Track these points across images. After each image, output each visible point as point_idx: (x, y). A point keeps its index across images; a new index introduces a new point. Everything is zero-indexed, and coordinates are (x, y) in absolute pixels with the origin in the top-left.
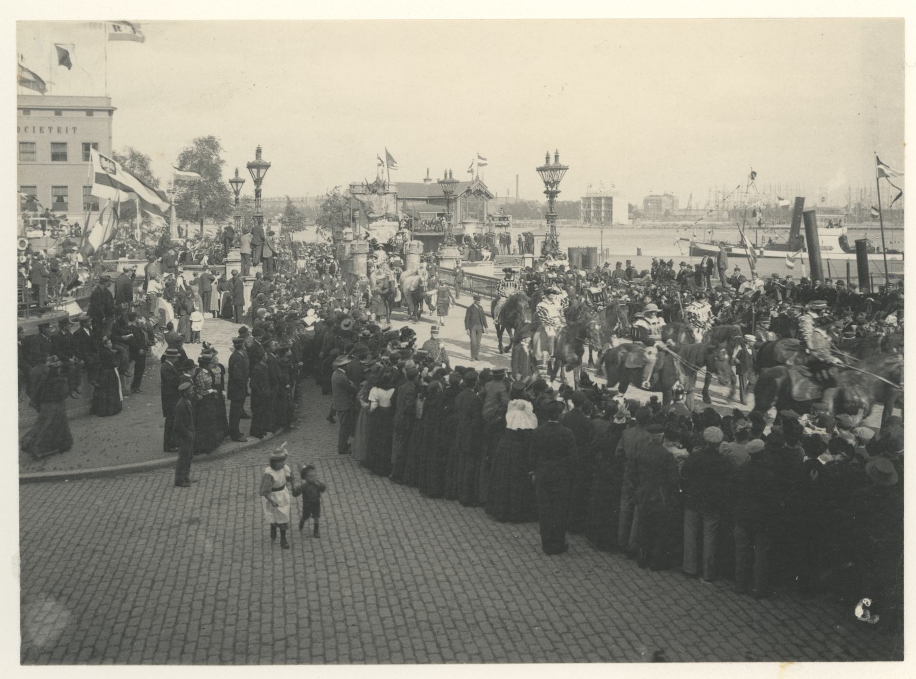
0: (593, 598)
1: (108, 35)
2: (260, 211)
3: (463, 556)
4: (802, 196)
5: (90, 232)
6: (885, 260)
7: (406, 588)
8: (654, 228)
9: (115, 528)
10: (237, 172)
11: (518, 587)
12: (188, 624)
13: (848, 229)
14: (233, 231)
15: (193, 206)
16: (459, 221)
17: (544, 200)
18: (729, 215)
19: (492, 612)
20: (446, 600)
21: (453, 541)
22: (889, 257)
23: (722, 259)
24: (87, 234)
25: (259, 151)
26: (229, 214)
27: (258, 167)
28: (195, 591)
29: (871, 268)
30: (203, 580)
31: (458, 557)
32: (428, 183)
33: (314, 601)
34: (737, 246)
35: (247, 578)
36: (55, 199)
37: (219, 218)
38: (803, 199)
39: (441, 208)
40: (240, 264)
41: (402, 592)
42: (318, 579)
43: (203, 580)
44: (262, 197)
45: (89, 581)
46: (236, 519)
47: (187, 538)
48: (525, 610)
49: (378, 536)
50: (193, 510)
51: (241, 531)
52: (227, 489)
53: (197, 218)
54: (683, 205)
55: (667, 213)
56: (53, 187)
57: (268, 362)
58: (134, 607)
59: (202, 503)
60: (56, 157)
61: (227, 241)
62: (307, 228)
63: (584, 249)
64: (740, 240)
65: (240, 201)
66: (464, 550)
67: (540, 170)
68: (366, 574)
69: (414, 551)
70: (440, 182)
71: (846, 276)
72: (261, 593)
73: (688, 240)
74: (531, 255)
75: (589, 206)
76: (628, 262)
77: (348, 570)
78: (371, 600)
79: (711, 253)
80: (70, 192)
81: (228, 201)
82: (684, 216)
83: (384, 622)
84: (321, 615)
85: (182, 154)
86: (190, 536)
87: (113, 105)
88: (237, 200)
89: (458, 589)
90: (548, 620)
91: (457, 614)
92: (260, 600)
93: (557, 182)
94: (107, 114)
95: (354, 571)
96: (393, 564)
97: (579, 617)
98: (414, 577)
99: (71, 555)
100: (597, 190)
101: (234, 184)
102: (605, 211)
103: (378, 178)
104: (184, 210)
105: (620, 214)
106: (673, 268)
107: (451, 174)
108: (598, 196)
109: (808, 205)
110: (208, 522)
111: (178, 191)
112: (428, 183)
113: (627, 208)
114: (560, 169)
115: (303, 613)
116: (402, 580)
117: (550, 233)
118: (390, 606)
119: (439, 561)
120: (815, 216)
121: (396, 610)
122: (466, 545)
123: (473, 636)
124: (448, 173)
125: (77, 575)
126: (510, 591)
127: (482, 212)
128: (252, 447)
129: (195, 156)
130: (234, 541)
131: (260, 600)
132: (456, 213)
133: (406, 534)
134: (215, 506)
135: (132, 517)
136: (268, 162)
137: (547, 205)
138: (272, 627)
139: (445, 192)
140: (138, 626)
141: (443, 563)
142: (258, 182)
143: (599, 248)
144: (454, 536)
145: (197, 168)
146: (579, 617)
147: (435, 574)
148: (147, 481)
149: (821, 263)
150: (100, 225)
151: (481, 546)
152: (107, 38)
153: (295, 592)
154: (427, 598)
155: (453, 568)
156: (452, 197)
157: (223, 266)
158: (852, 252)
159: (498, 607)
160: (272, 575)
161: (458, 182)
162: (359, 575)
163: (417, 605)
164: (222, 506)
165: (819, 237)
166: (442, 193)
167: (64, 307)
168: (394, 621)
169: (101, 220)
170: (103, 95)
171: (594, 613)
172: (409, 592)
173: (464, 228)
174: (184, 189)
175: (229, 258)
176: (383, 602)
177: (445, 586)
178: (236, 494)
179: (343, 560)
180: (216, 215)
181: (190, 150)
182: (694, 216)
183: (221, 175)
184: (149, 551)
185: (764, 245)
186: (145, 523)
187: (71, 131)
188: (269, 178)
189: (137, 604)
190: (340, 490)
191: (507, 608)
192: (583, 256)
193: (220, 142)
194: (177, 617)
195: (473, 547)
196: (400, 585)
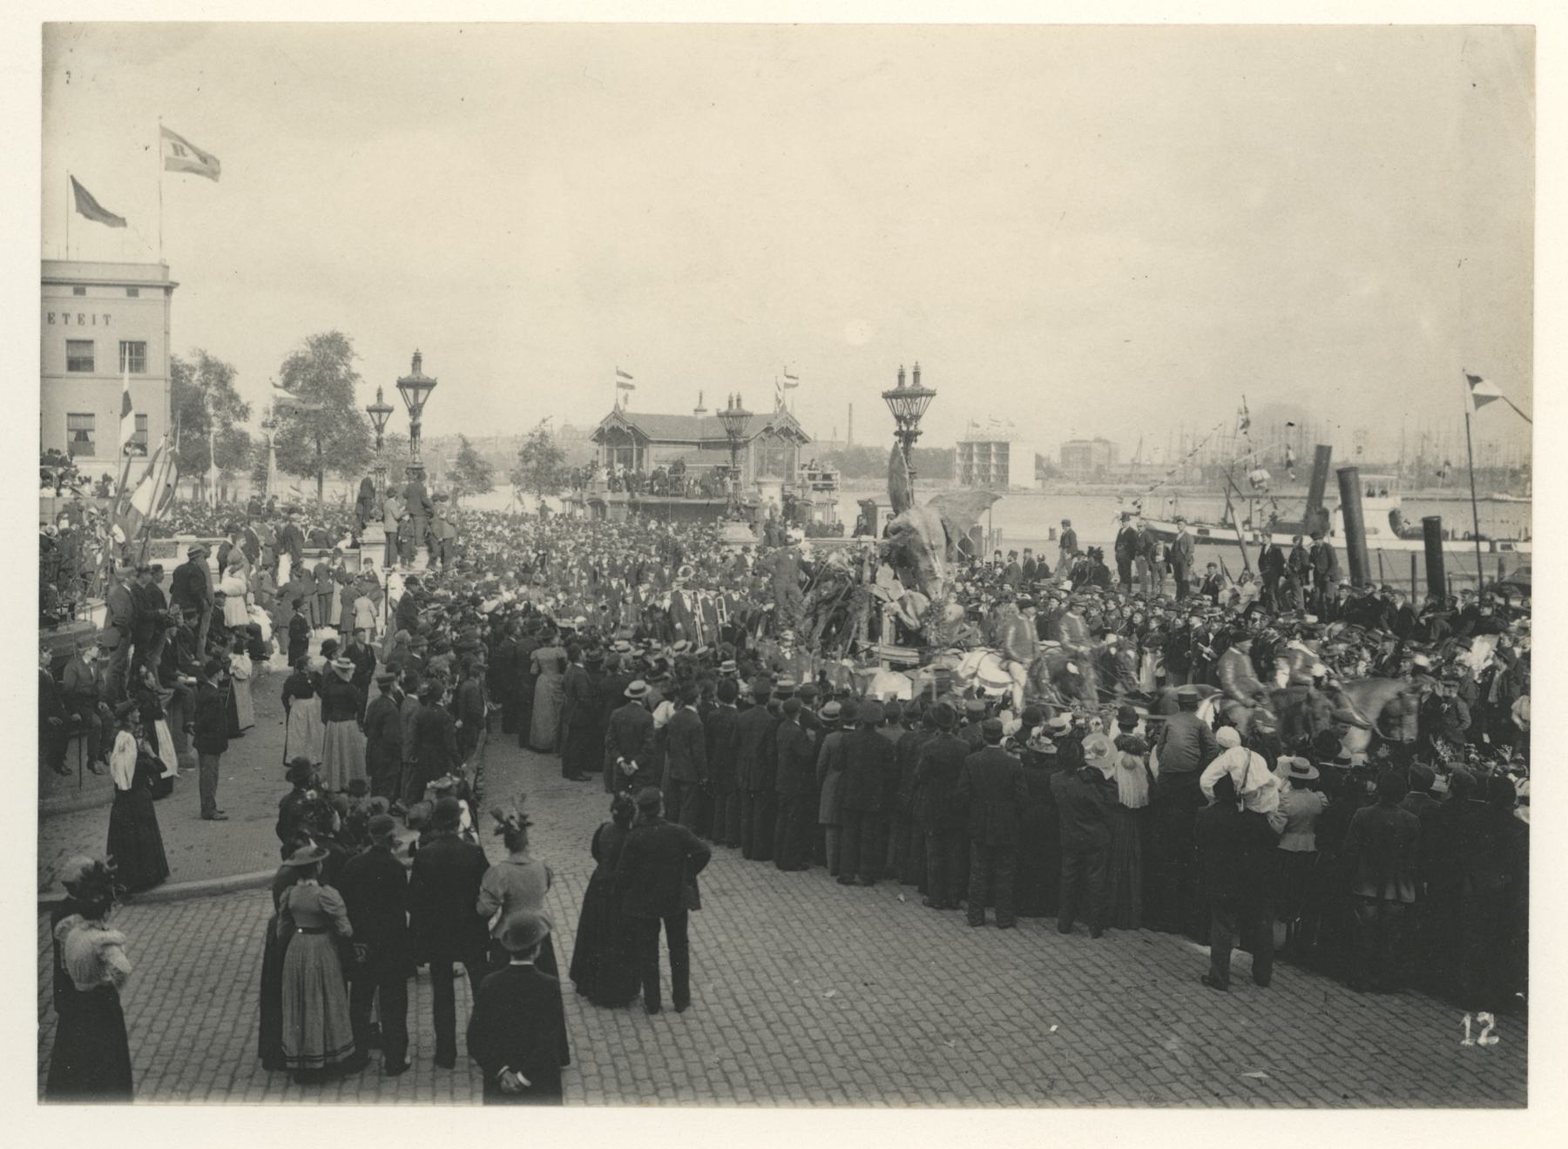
9: (170, 988)
10: (380, 394)
13: (1403, 500)
15: (305, 450)
16: (751, 479)
18: (1203, 476)
21: (735, 1013)
24: (123, 491)
25: (417, 359)
26: (366, 463)
27: (416, 385)
31: (744, 1042)
32: (701, 416)
36: (73, 435)
37: (348, 471)
38: (1330, 448)
39: (722, 457)
44: (422, 436)
53: (311, 470)
54: (1125, 458)
60: (74, 365)
64: (1222, 516)
65: (385, 443)
66: (754, 1031)
67: (887, 396)
69: (670, 1030)
70: (720, 416)
71: (1409, 576)
74: (871, 538)
75: (970, 457)
79: (1169, 537)
80: (98, 422)
81: (365, 441)
82: (1129, 476)
85: (289, 362)
87: (172, 277)
88: (379, 442)
93: (917, 417)
94: (162, 291)
101: (375, 415)
102: (997, 466)
103: (617, 406)
104: (293, 462)
105: (1021, 472)
108: (985, 440)
109: (1337, 459)
111: (281, 424)
113: (1033, 460)
114: (922, 395)
120: (1357, 478)
124: (735, 399)
127: (790, 467)
129: (310, 366)
132: (747, 467)
135: (197, 971)
139: (729, 432)
142: (415, 411)
144: (739, 1006)
148: (223, 909)
152: (163, 165)
156: (741, 440)
161: (751, 415)
166: (725, 434)
167: (88, 616)
170: (156, 261)
173: (760, 491)
181: (300, 355)
182: (1144, 476)
183: (352, 398)
184: (226, 1027)
186: (220, 980)
187: (100, 320)
188: (433, 404)
195: (769, 1025)
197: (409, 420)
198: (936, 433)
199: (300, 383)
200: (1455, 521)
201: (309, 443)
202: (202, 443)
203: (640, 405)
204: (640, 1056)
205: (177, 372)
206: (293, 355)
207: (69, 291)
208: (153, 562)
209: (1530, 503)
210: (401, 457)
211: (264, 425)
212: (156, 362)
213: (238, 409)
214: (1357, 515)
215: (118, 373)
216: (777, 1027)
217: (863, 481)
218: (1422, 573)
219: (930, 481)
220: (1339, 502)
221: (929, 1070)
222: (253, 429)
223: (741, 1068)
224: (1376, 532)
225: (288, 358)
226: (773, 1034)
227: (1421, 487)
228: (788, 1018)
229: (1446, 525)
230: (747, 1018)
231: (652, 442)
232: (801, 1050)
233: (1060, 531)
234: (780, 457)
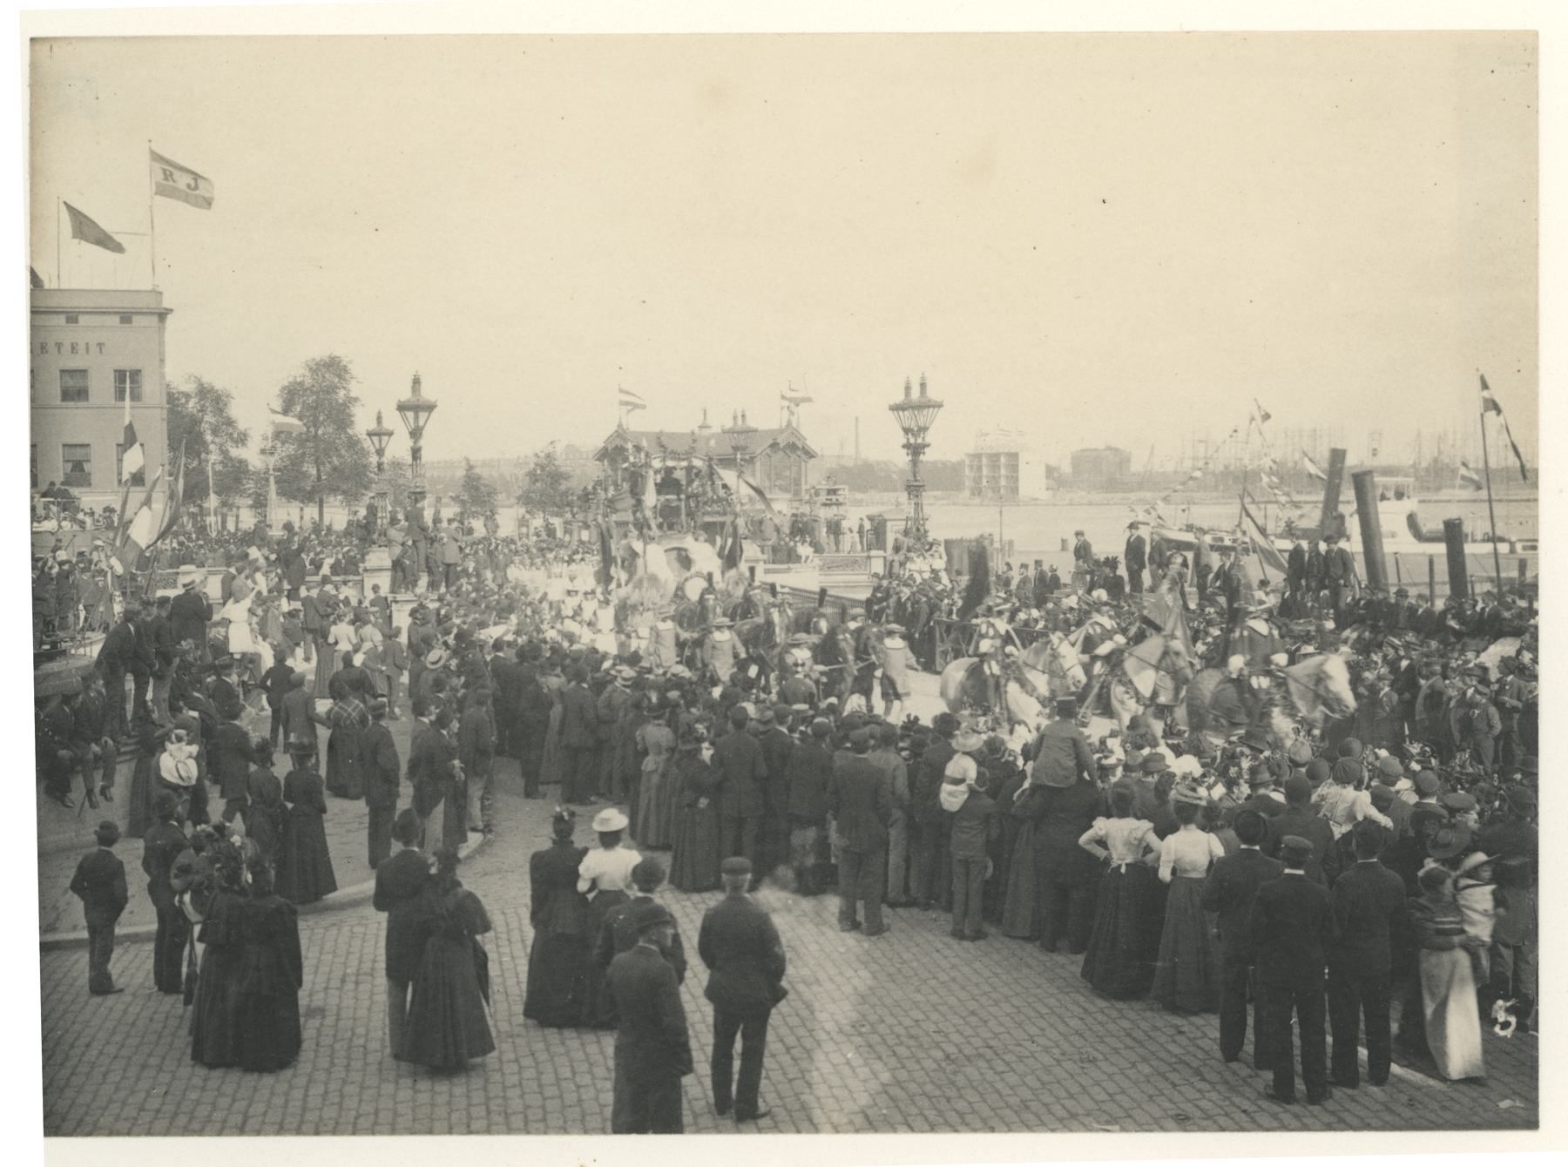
1: (154, 188)
4: (1339, 446)
5: (131, 522)
8: (1090, 504)
10: (379, 419)
15: (305, 475)
17: (902, 459)
25: (416, 382)
26: (366, 488)
27: (416, 408)
29: (1471, 568)
32: (706, 432)
36: (70, 465)
37: (351, 497)
38: (1344, 452)
40: (389, 574)
42: (527, 1107)
44: (423, 460)
45: (136, 1119)
52: (372, 957)
54: (1136, 466)
56: (64, 446)
59: (329, 980)
60: (67, 395)
63: (970, 541)
67: (896, 408)
71: (1427, 580)
73: (1147, 524)
74: (881, 553)
75: (980, 468)
76: (1038, 563)
79: (1188, 546)
80: (95, 452)
85: (284, 388)
87: (166, 304)
88: (380, 465)
93: (924, 429)
94: (155, 319)
99: (105, 1075)
101: (375, 439)
102: (1007, 477)
103: (620, 425)
104: (292, 485)
105: (1032, 482)
109: (1352, 461)
110: (338, 1014)
111: (279, 450)
117: (912, 515)
125: (115, 1108)
127: (797, 482)
134: (350, 986)
136: (433, 400)
137: (908, 468)
142: (416, 434)
143: (996, 538)
149: (1383, 563)
161: (756, 431)
162: (597, 1099)
164: (361, 987)
167: (88, 649)
169: (147, 502)
174: (291, 449)
175: (368, 565)
181: (299, 380)
185: (1279, 531)
187: (94, 349)
193: (350, 366)
195: (788, 1050)
197: (410, 443)
198: (944, 445)
199: (299, 408)
202: (201, 471)
203: (638, 423)
205: (172, 398)
206: (291, 379)
207: (62, 319)
210: (401, 481)
211: (263, 452)
213: (235, 436)
214: (1373, 516)
217: (875, 495)
219: (938, 493)
220: (1355, 506)
221: (952, 1093)
222: (251, 455)
224: (1393, 535)
225: (286, 384)
229: (1467, 528)
233: (1073, 543)
234: (787, 473)
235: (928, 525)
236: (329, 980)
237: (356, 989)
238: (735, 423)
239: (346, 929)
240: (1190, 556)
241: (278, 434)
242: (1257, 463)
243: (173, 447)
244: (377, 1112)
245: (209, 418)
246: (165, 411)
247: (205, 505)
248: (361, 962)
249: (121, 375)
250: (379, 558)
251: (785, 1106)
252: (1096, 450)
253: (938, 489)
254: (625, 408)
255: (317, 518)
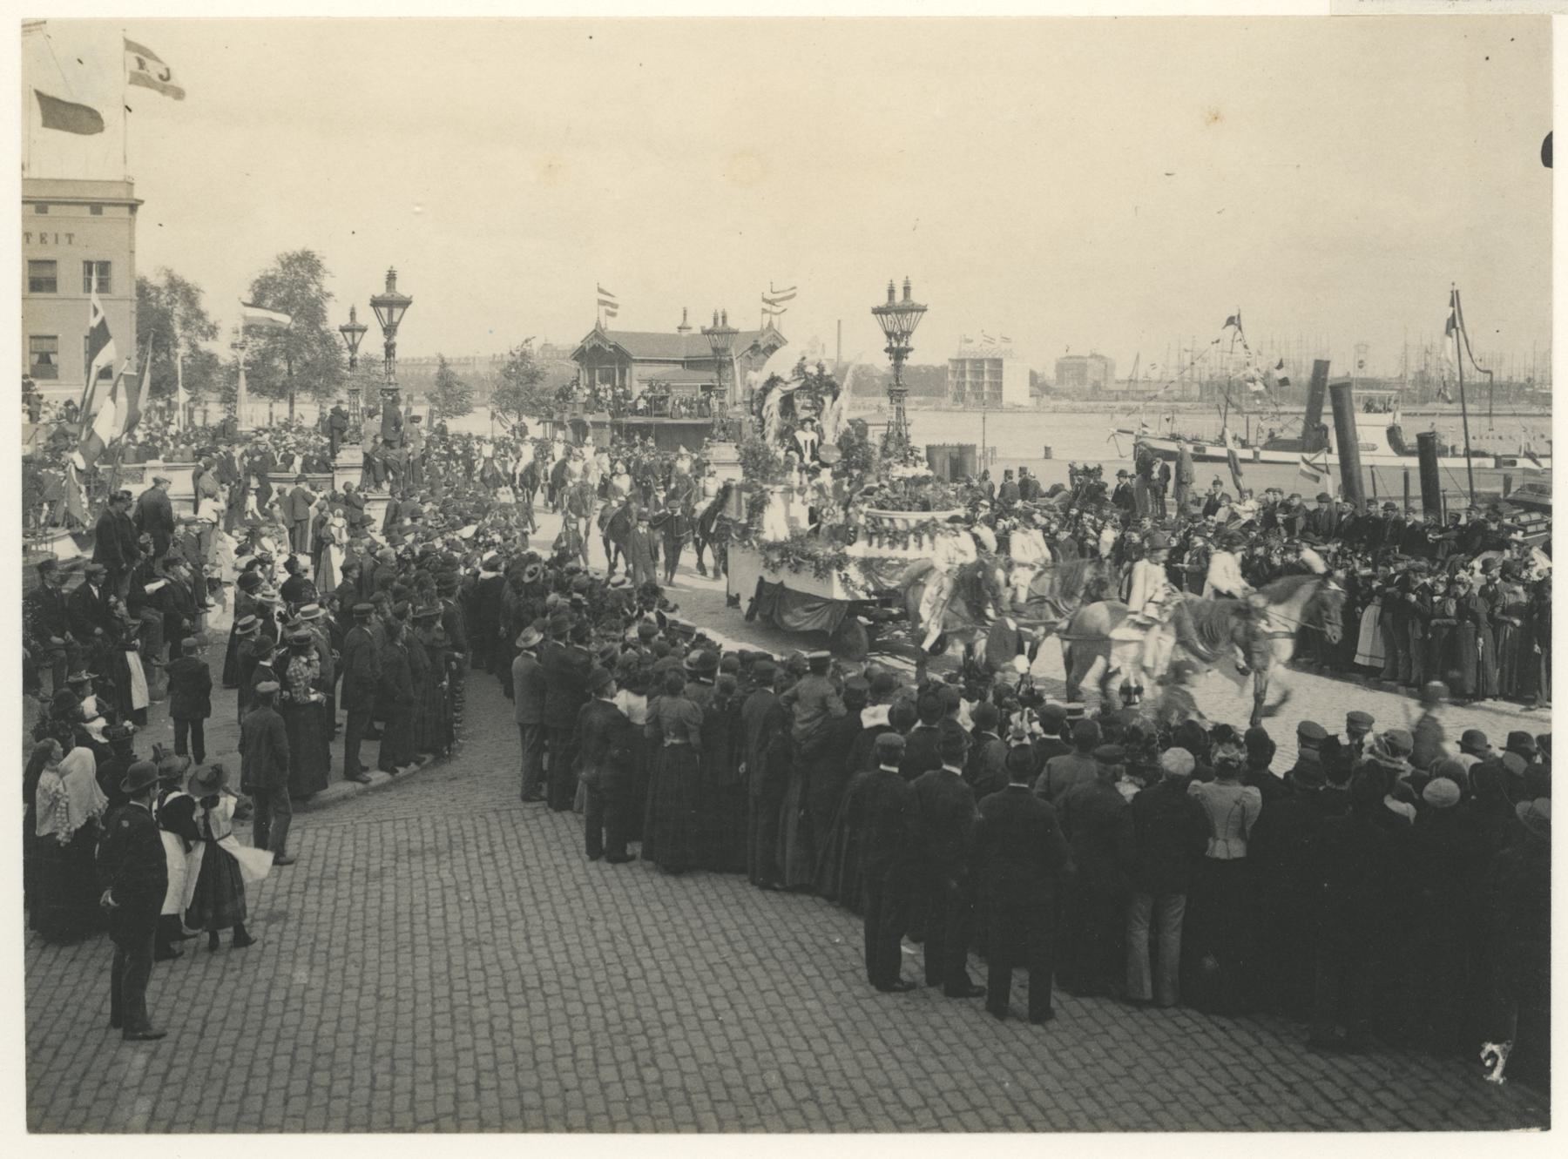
0: (968, 1047)
2: (393, 380)
3: (743, 975)
4: (1325, 358)
5: (95, 415)
6: (1469, 468)
7: (644, 1032)
8: (1074, 411)
10: (353, 314)
11: (839, 1030)
12: (265, 1096)
13: (1403, 415)
14: (345, 416)
15: (275, 370)
17: (884, 363)
19: (793, 1072)
20: (714, 1052)
21: (726, 950)
22: (1475, 462)
23: (1185, 466)
24: (89, 419)
25: (391, 277)
26: (339, 384)
27: (390, 304)
28: (278, 1038)
29: (1444, 482)
30: (292, 1018)
33: (486, 1054)
34: (1214, 444)
35: (368, 1016)
36: (36, 358)
37: (322, 393)
38: (1328, 363)
39: (708, 377)
41: (637, 1038)
42: (493, 1016)
43: (292, 1018)
44: (397, 358)
46: (350, 912)
47: (264, 946)
48: (851, 1069)
49: (597, 943)
50: (274, 897)
51: (358, 934)
52: (336, 860)
53: (282, 392)
54: (1121, 373)
55: (1096, 387)
57: (407, 643)
58: (171, 1066)
59: (291, 885)
61: (336, 432)
62: (475, 409)
63: (953, 447)
64: (1220, 433)
65: (359, 363)
66: (745, 967)
67: (877, 311)
68: (575, 1008)
70: (707, 333)
71: (1402, 494)
72: (394, 1042)
73: (1132, 433)
75: (963, 374)
76: (1023, 470)
77: (546, 1001)
78: (585, 1053)
79: (1169, 455)
81: (339, 362)
82: (1126, 392)
83: (607, 1091)
84: (498, 1078)
85: (257, 281)
86: (269, 943)
87: (137, 195)
88: (353, 362)
89: (735, 1032)
90: (890, 1085)
91: (733, 1076)
92: (391, 1053)
93: (908, 333)
94: (127, 209)
95: (555, 1003)
96: (624, 990)
97: (942, 1080)
98: (659, 1012)
99: (61, 979)
100: (979, 348)
101: (348, 335)
103: (598, 324)
104: (263, 382)
105: (1015, 389)
106: (1104, 479)
107: (724, 317)
109: (1336, 373)
110: (301, 918)
111: (250, 344)
112: (685, 333)
113: (1027, 377)
114: (912, 311)
115: (467, 1076)
116: (639, 1017)
117: (894, 419)
118: (618, 1064)
119: (703, 985)
120: (1350, 394)
121: (629, 1070)
122: (749, 958)
123: (759, 1114)
124: (720, 315)
126: (825, 1037)
128: (383, 788)
130: (347, 952)
131: (391, 1053)
133: (646, 938)
137: (891, 373)
138: (412, 1100)
139: (715, 350)
140: (178, 1099)
141: (710, 989)
142: (390, 330)
143: (979, 445)
144: (730, 942)
145: (284, 305)
146: (942, 1080)
147: (696, 1007)
149: (1360, 471)
150: (111, 403)
151: (775, 958)
153: (453, 1039)
154: (681, 1048)
155: (726, 996)
157: (329, 475)
158: (1410, 454)
159: (804, 1063)
160: (413, 1011)
161: (736, 332)
162: (564, 1009)
163: (663, 1061)
164: (325, 891)
165: (1358, 428)
166: (710, 352)
167: (49, 546)
168: (624, 1088)
169: (113, 395)
170: (121, 178)
171: (971, 1077)
172: (650, 1039)
176: (605, 1057)
177: (713, 1027)
178: (349, 869)
179: (537, 984)
180: (316, 388)
181: (271, 274)
182: (1142, 392)
183: (324, 319)
185: (1262, 442)
187: (63, 240)
189: (176, 1061)
190: (532, 862)
191: (820, 1066)
192: (951, 458)
193: (323, 262)
194: (247, 1083)
195: (760, 961)
196: (636, 1026)
198: (928, 350)
200: (1449, 432)
201: (280, 363)
202: (169, 365)
204: (628, 994)
205: (142, 289)
208: (124, 487)
209: (1550, 415)
210: (375, 378)
211: (234, 346)
212: (122, 285)
213: (205, 329)
215: (82, 295)
216: (770, 963)
218: (1416, 489)
219: (922, 398)
222: (222, 349)
223: (732, 1005)
226: (765, 969)
227: (1425, 401)
228: (781, 954)
230: (738, 954)
231: (635, 361)
232: (794, 987)
235: (910, 430)
236: (291, 885)
237: (320, 893)
238: (715, 322)
239: (310, 833)
240: (1172, 465)
241: (248, 329)
242: (1243, 372)
243: (142, 340)
244: (339, 1019)
245: (179, 310)
246: (134, 304)
247: (174, 400)
248: (325, 866)
249: (88, 265)
250: (351, 455)
251: (756, 1018)
252: (1082, 357)
253: (920, 394)
254: (603, 309)
255: (287, 415)
